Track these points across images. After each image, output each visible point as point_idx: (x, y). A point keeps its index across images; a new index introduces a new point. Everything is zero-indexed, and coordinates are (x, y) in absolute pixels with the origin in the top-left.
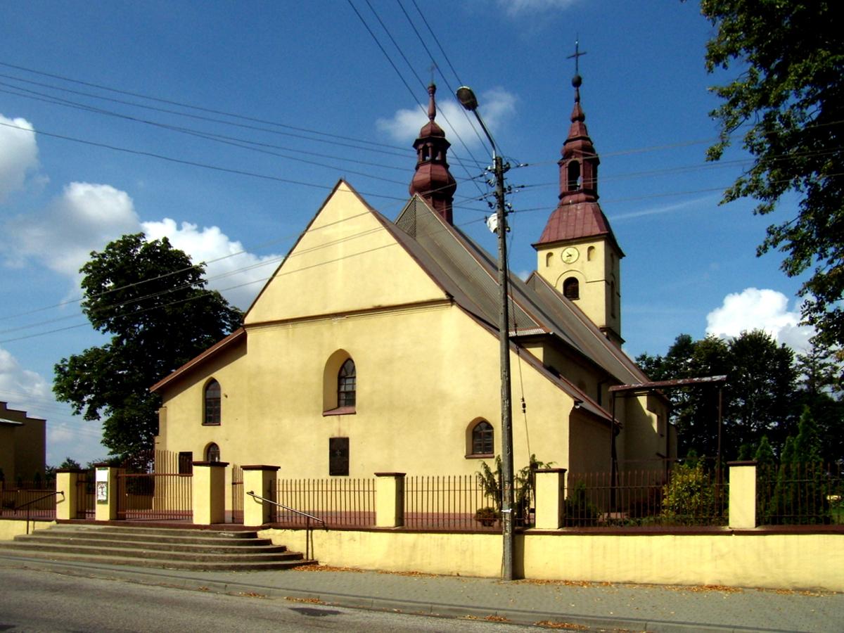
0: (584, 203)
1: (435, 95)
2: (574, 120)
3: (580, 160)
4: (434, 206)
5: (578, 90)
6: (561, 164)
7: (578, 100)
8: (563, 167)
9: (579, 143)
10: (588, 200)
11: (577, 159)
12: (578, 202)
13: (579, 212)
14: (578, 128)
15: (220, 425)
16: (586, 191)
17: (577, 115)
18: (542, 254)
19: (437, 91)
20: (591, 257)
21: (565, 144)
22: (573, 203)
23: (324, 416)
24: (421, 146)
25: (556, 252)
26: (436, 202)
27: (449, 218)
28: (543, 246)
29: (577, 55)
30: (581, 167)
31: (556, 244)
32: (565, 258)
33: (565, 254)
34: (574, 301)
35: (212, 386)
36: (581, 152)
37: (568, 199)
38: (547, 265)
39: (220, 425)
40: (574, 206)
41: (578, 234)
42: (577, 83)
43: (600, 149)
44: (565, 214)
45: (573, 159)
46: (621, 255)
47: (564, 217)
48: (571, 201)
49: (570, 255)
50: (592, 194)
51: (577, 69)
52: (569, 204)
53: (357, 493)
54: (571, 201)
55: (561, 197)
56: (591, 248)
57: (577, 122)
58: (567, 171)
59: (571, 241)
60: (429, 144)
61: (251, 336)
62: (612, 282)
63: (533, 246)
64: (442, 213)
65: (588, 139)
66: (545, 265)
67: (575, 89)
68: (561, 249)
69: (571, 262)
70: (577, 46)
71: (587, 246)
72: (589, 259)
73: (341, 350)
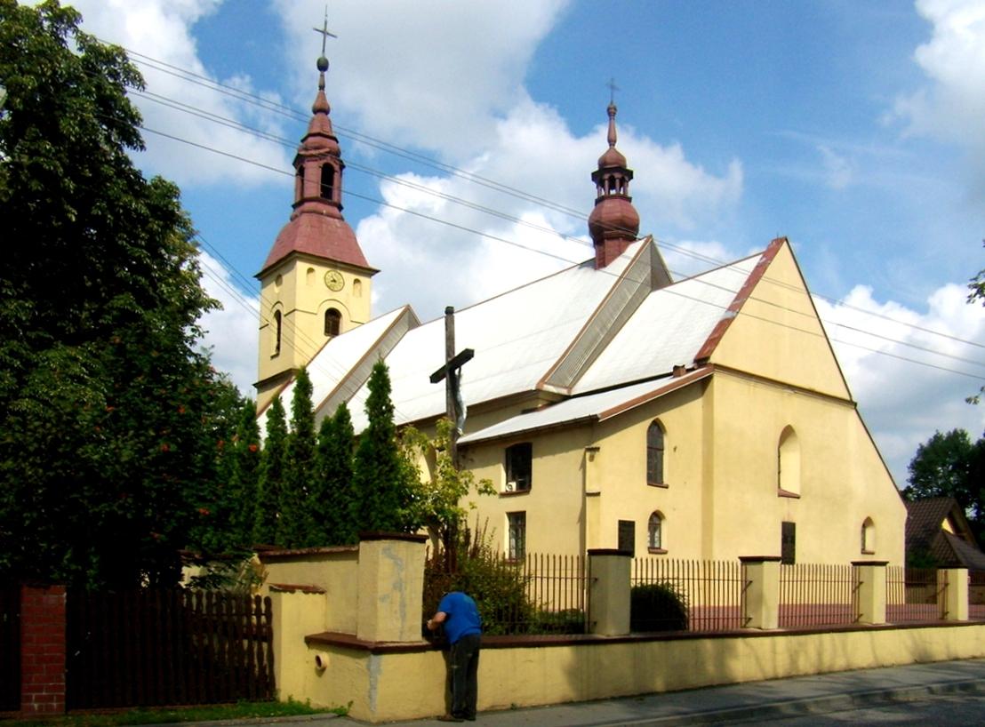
5: (322, 76)
7: (322, 87)
11: (332, 163)
13: (339, 230)
28: (305, 257)
45: (328, 160)
48: (324, 212)
49: (334, 281)
51: (324, 51)
53: (557, 581)
59: (339, 265)
61: (719, 381)
67: (319, 72)
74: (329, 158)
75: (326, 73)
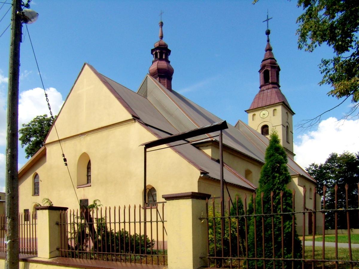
0: (271, 89)
1: (163, 27)
2: (266, 51)
3: (269, 69)
4: (160, 82)
5: (268, 37)
6: (260, 71)
7: (268, 41)
8: (261, 73)
9: (269, 61)
10: (273, 88)
11: (268, 69)
12: (268, 89)
14: (268, 54)
15: (39, 195)
16: (272, 83)
17: (268, 48)
18: (250, 115)
19: (164, 25)
20: (275, 114)
21: (262, 62)
22: (266, 90)
23: (78, 188)
24: (154, 53)
25: (257, 113)
26: (161, 80)
27: (169, 88)
28: (250, 111)
29: (268, 20)
30: (270, 72)
31: (257, 109)
32: (261, 116)
33: (262, 114)
34: (267, 136)
35: (36, 176)
36: (270, 65)
37: (263, 88)
38: (253, 120)
39: (39, 195)
40: (266, 91)
41: (268, 103)
42: (268, 33)
43: (279, 63)
44: (262, 95)
45: (266, 68)
46: (293, 113)
47: (261, 97)
48: (265, 89)
49: (264, 114)
50: (276, 84)
52: (264, 90)
54: (265, 89)
55: (260, 88)
56: (275, 110)
57: (268, 52)
58: (263, 75)
59: (264, 108)
60: (158, 51)
62: (287, 126)
63: (246, 111)
64: (164, 85)
65: (274, 59)
66: (252, 120)
67: (267, 36)
68: (260, 112)
69: (265, 117)
70: (268, 16)
71: (272, 109)
72: (274, 115)
73: (84, 152)
74: (266, 68)
75: (269, 35)
